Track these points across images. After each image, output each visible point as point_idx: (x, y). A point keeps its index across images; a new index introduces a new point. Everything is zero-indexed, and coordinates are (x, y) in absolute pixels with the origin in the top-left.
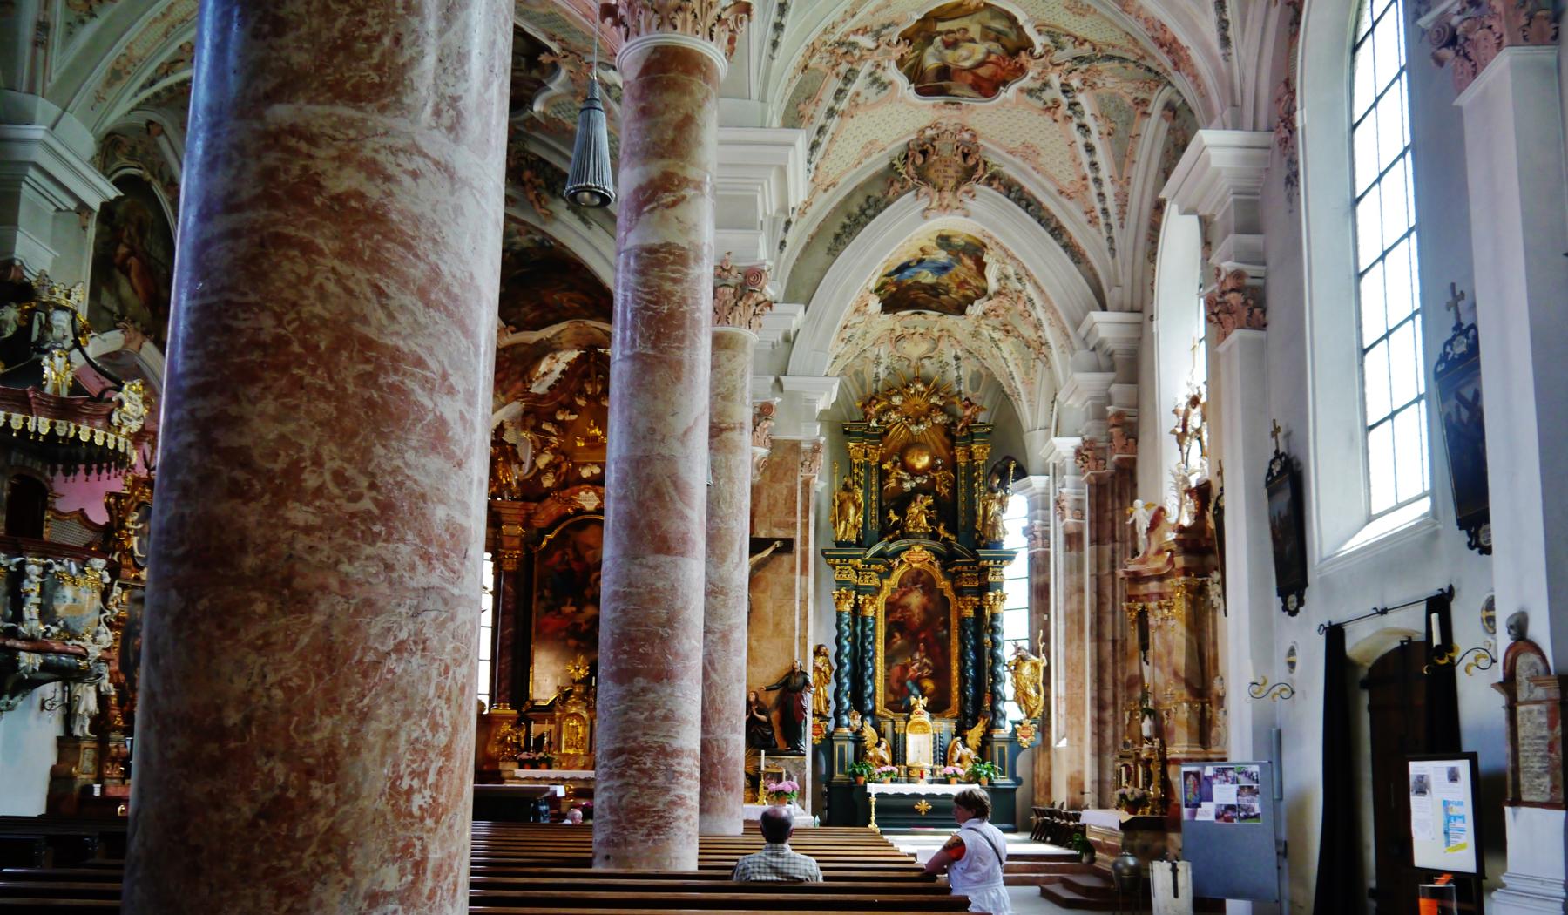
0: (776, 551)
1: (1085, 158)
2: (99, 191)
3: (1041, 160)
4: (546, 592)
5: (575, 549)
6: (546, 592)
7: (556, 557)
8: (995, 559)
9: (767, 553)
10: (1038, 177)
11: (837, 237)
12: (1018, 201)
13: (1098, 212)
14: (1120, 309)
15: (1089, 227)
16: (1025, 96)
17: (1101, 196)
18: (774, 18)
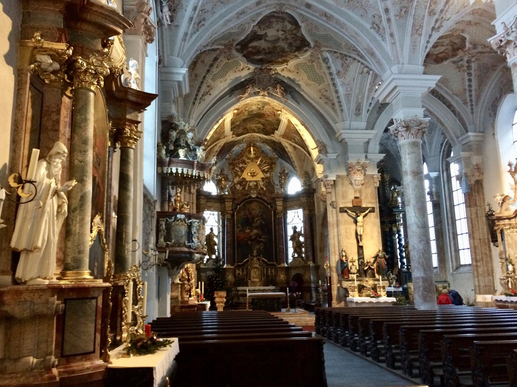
0: (370, 212)
1: (467, 83)
2: (186, 91)
3: (449, 84)
4: (239, 225)
5: (249, 210)
6: (239, 225)
7: (242, 213)
8: (398, 212)
9: (367, 212)
10: (446, 89)
11: (380, 108)
12: (436, 96)
13: (468, 101)
14: (475, 132)
15: (463, 105)
16: (452, 64)
17: (471, 96)
18: (427, 39)
